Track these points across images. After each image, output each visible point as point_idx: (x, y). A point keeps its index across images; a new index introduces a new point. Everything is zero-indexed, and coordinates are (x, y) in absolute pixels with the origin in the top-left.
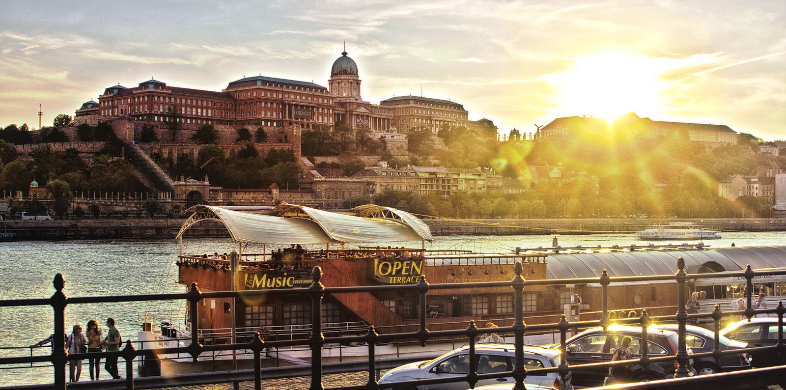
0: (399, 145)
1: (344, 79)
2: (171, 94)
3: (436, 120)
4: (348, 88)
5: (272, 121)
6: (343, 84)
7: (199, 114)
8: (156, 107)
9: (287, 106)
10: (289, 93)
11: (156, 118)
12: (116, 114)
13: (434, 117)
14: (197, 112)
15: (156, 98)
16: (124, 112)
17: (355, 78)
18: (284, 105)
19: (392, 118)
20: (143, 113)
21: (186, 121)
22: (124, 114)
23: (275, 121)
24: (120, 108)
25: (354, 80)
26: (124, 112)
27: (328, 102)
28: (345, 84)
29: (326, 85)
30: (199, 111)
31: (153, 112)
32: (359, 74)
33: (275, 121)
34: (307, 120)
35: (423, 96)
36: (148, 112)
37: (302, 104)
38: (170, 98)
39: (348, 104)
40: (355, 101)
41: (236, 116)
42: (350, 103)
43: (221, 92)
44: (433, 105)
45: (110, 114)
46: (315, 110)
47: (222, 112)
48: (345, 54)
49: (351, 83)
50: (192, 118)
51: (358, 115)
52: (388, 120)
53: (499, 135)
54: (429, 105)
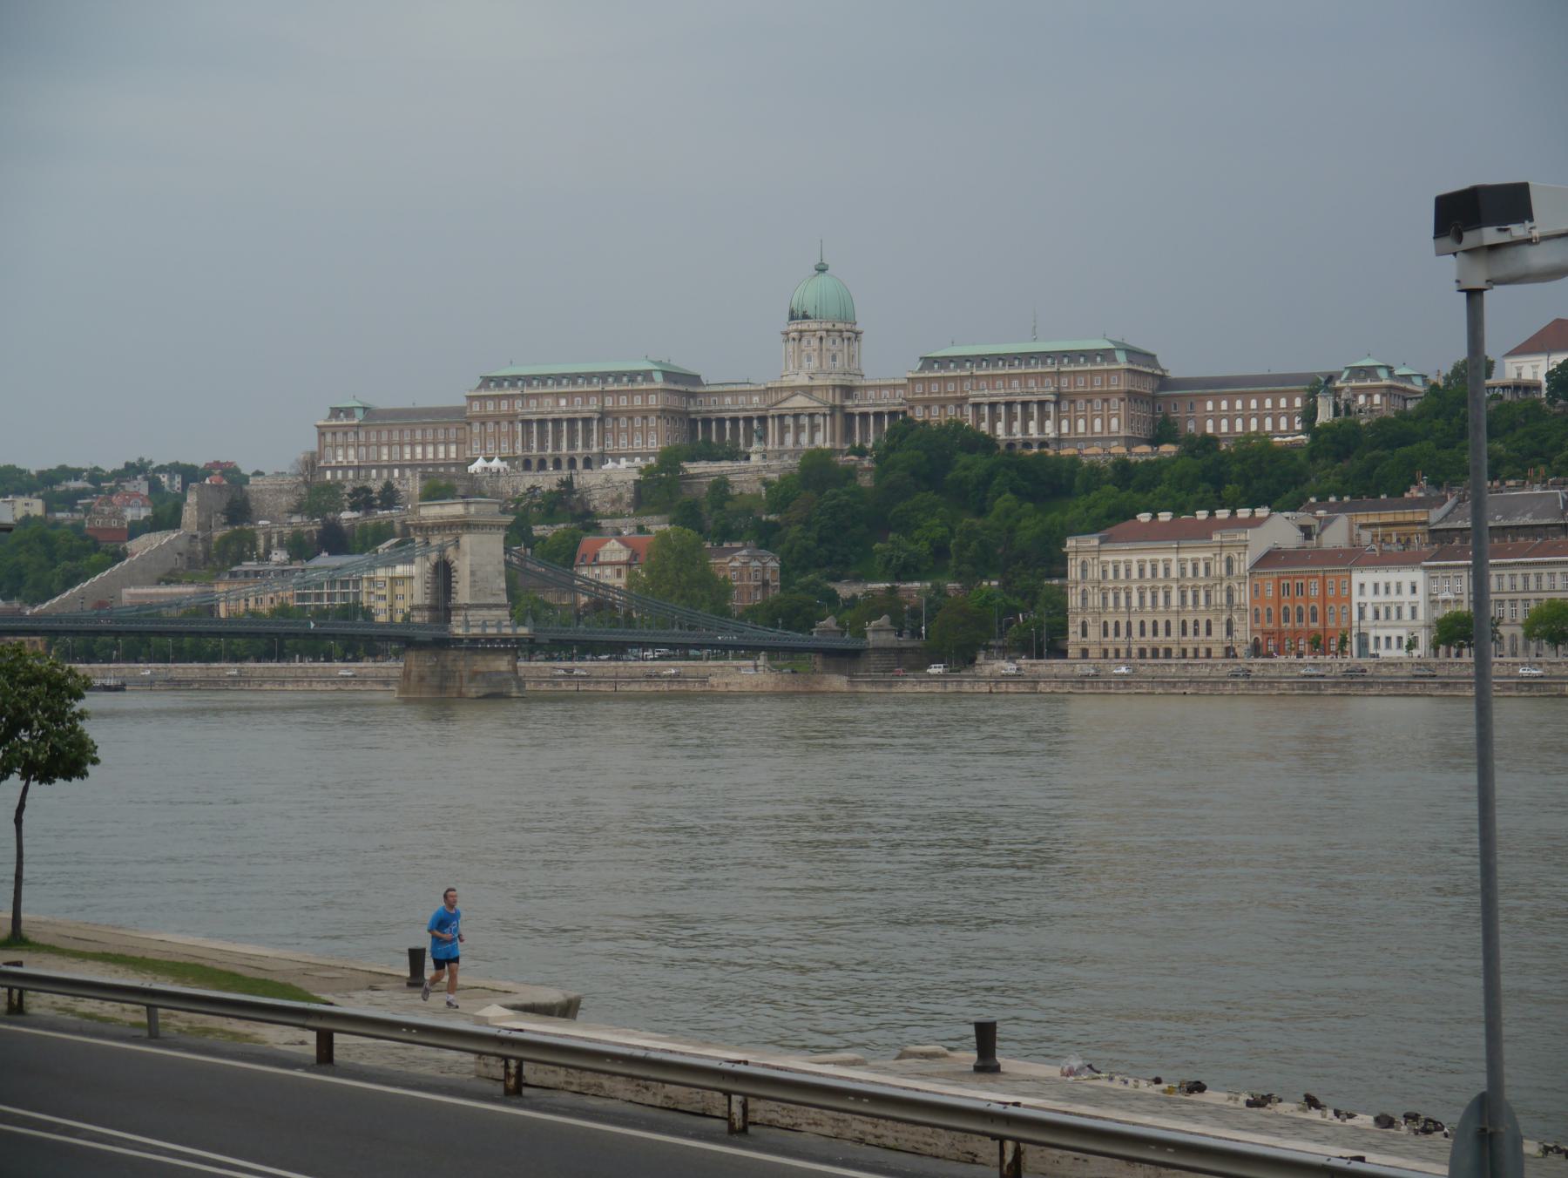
2: (358, 426)
14: (413, 453)
17: (814, 326)
38: (357, 434)
44: (979, 366)
50: (402, 467)
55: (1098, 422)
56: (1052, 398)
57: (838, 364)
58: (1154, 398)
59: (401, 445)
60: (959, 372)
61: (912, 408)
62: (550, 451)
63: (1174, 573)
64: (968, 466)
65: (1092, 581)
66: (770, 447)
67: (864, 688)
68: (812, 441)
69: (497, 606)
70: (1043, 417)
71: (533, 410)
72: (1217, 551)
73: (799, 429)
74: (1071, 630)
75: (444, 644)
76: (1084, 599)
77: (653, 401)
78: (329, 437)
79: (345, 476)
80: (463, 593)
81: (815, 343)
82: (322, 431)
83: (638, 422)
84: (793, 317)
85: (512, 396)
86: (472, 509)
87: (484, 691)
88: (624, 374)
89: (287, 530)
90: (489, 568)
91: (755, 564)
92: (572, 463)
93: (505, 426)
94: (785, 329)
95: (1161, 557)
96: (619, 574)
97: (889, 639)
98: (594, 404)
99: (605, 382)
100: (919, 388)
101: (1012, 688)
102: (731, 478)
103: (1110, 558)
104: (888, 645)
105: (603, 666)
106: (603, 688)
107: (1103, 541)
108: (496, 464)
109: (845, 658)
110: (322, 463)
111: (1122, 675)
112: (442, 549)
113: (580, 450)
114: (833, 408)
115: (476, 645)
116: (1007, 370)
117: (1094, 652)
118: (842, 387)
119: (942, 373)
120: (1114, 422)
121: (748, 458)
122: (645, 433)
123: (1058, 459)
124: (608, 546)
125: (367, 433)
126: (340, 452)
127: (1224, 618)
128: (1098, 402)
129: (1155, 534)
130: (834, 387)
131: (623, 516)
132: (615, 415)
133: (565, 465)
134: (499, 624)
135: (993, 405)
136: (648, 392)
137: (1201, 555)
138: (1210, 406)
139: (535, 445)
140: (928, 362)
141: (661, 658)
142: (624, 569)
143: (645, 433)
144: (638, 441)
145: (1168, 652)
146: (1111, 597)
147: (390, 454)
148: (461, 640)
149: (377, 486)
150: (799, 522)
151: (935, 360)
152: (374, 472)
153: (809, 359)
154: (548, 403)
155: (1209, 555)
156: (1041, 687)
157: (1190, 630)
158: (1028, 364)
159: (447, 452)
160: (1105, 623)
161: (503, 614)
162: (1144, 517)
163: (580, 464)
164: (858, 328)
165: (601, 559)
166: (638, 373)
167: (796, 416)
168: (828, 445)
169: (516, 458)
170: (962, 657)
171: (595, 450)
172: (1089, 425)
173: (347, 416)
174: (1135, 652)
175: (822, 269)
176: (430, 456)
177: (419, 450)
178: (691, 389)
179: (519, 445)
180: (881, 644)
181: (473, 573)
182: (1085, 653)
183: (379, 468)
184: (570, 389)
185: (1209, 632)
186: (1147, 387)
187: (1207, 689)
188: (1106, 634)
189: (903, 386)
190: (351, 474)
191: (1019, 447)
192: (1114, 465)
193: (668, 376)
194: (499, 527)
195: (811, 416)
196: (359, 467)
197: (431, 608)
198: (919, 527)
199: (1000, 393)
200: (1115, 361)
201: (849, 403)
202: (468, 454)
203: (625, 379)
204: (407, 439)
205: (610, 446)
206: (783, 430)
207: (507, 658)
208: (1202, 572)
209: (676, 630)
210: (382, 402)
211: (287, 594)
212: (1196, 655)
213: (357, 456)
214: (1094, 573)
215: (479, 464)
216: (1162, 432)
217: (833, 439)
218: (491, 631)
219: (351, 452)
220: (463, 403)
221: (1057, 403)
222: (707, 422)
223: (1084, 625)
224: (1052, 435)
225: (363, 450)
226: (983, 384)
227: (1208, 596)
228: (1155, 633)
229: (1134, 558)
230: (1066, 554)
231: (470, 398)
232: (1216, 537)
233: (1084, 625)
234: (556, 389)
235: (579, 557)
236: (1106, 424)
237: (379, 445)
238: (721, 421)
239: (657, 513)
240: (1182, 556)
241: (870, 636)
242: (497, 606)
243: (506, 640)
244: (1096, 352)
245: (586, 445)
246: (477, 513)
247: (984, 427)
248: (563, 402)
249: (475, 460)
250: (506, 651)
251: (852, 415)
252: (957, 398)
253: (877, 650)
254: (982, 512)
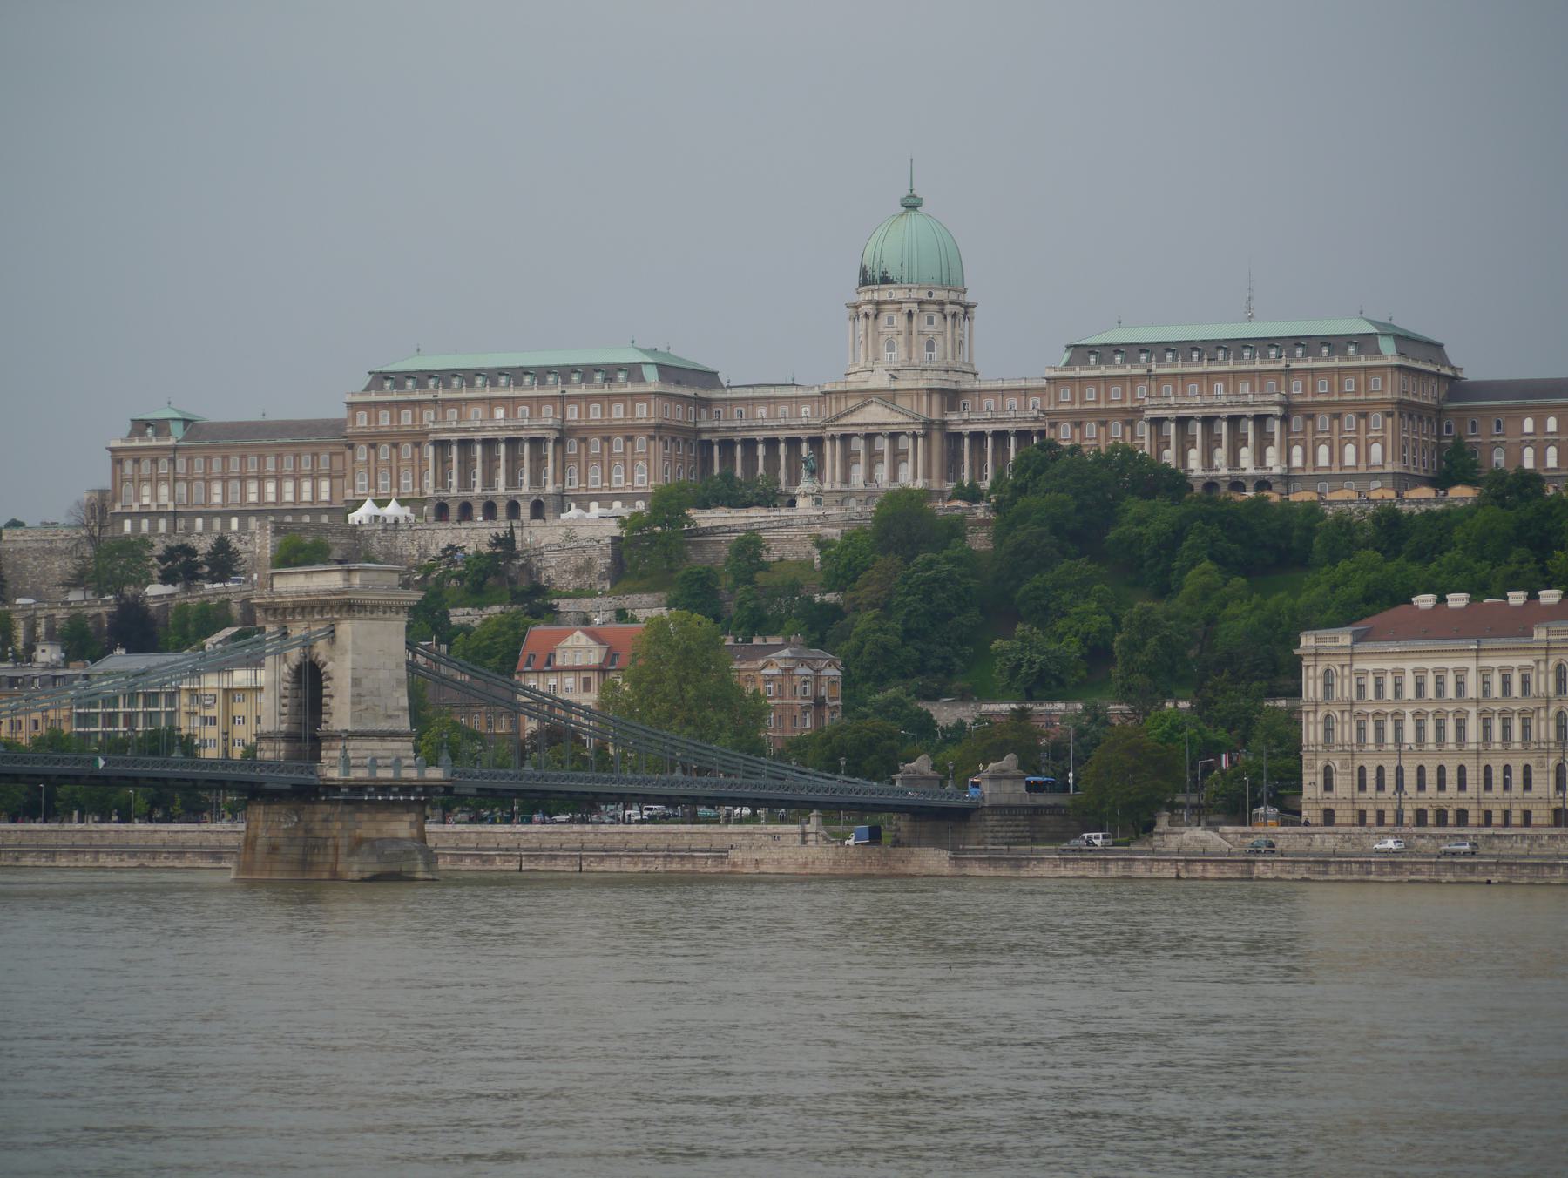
0: (581, 561)
2: (175, 449)
14: (261, 492)
17: (899, 295)
37: (489, 435)
38: (173, 461)
44: (1161, 360)
50: (243, 514)
55: (1350, 450)
56: (1277, 410)
57: (935, 354)
58: (1440, 412)
59: (243, 479)
60: (1129, 370)
61: (1054, 425)
62: (478, 490)
63: (1472, 690)
64: (1144, 518)
65: (1341, 701)
66: (827, 487)
67: (975, 869)
68: (894, 477)
69: (394, 735)
70: (1263, 441)
71: (451, 424)
72: (1541, 655)
73: (873, 458)
74: (1306, 779)
75: (308, 794)
76: (1328, 731)
77: (642, 412)
78: (128, 467)
79: (154, 527)
80: (340, 715)
81: (900, 321)
82: (117, 457)
83: (618, 444)
84: (865, 280)
85: (419, 403)
86: (356, 580)
87: (373, 868)
88: (596, 369)
89: (61, 614)
90: (383, 674)
91: (802, 670)
92: (513, 509)
93: (407, 450)
94: (855, 299)
95: (1450, 664)
96: (587, 685)
97: (1013, 792)
98: (549, 416)
99: (566, 381)
100: (1065, 394)
101: (1212, 871)
102: (765, 536)
103: (1370, 666)
104: (1015, 801)
105: (560, 832)
106: (560, 866)
107: (1359, 638)
108: (392, 510)
109: (946, 821)
110: (118, 508)
111: (1388, 852)
112: (307, 644)
113: (525, 489)
114: (928, 424)
115: (361, 797)
116: (1206, 367)
117: (1344, 815)
118: (942, 391)
119: (1103, 371)
120: (1376, 449)
121: (792, 504)
122: (630, 463)
123: (1287, 509)
124: (570, 642)
125: (189, 459)
126: (146, 490)
127: (1552, 762)
128: (1350, 419)
129: (1441, 628)
130: (930, 391)
131: (593, 595)
132: (582, 434)
133: (502, 512)
134: (397, 764)
135: (1182, 422)
136: (635, 397)
137: (1516, 662)
138: (1529, 425)
139: (455, 480)
140: (1081, 352)
141: (652, 820)
142: (594, 678)
143: (630, 463)
144: (618, 476)
145: (1462, 817)
146: (1371, 727)
147: (225, 494)
148: (336, 789)
149: (203, 545)
150: (874, 606)
151: (1091, 349)
152: (199, 522)
153: (891, 348)
154: (476, 414)
155: (1529, 662)
156: (1259, 869)
157: (1497, 780)
158: (1239, 357)
159: (315, 491)
160: (1362, 769)
161: (404, 747)
162: (1425, 601)
163: (525, 512)
164: (968, 299)
165: (559, 662)
166: (620, 368)
167: (870, 438)
168: (919, 484)
169: (424, 501)
170: (1135, 822)
171: (550, 489)
172: (1337, 455)
173: (157, 434)
174: (1409, 815)
175: (911, 205)
176: (289, 497)
177: (271, 487)
178: (703, 394)
179: (429, 481)
180: (1003, 800)
181: (356, 682)
182: (1329, 817)
183: (208, 515)
184: (511, 392)
185: (1527, 785)
186: (1428, 395)
187: (1525, 876)
188: (1362, 786)
189: (1040, 391)
190: (162, 525)
191: (1224, 488)
192: (1377, 519)
193: (666, 372)
194: (399, 609)
195: (894, 437)
196: (176, 515)
197: (289, 737)
198: (1065, 614)
199: (1194, 403)
200: (1378, 352)
201: (953, 417)
202: (349, 497)
203: (598, 377)
204: (252, 470)
205: (574, 484)
206: (848, 459)
207: (411, 817)
208: (1516, 690)
209: (678, 774)
210: (214, 411)
211: (61, 715)
212: (1507, 822)
213: (173, 495)
214: (1345, 688)
215: (365, 512)
216: (1453, 466)
217: (928, 475)
218: (385, 774)
219: (164, 490)
220: (342, 413)
221: (1285, 419)
222: (727, 446)
223: (1328, 772)
224: (1277, 470)
225: (182, 488)
226: (1167, 388)
227: (1526, 728)
228: (1441, 786)
229: (1409, 666)
230: (1300, 658)
231: (350, 405)
232: (1540, 634)
233: (1328, 772)
234: (488, 393)
235: (523, 659)
236: (1363, 454)
237: (208, 480)
238: (750, 445)
239: (647, 590)
240: (1484, 663)
241: (987, 787)
242: (394, 735)
243: (407, 789)
244: (1349, 339)
245: (536, 480)
246: (364, 586)
247: (1169, 456)
248: (500, 413)
249: (360, 503)
250: (407, 806)
251: (958, 436)
252: (1125, 410)
253: (996, 809)
254: (1164, 591)
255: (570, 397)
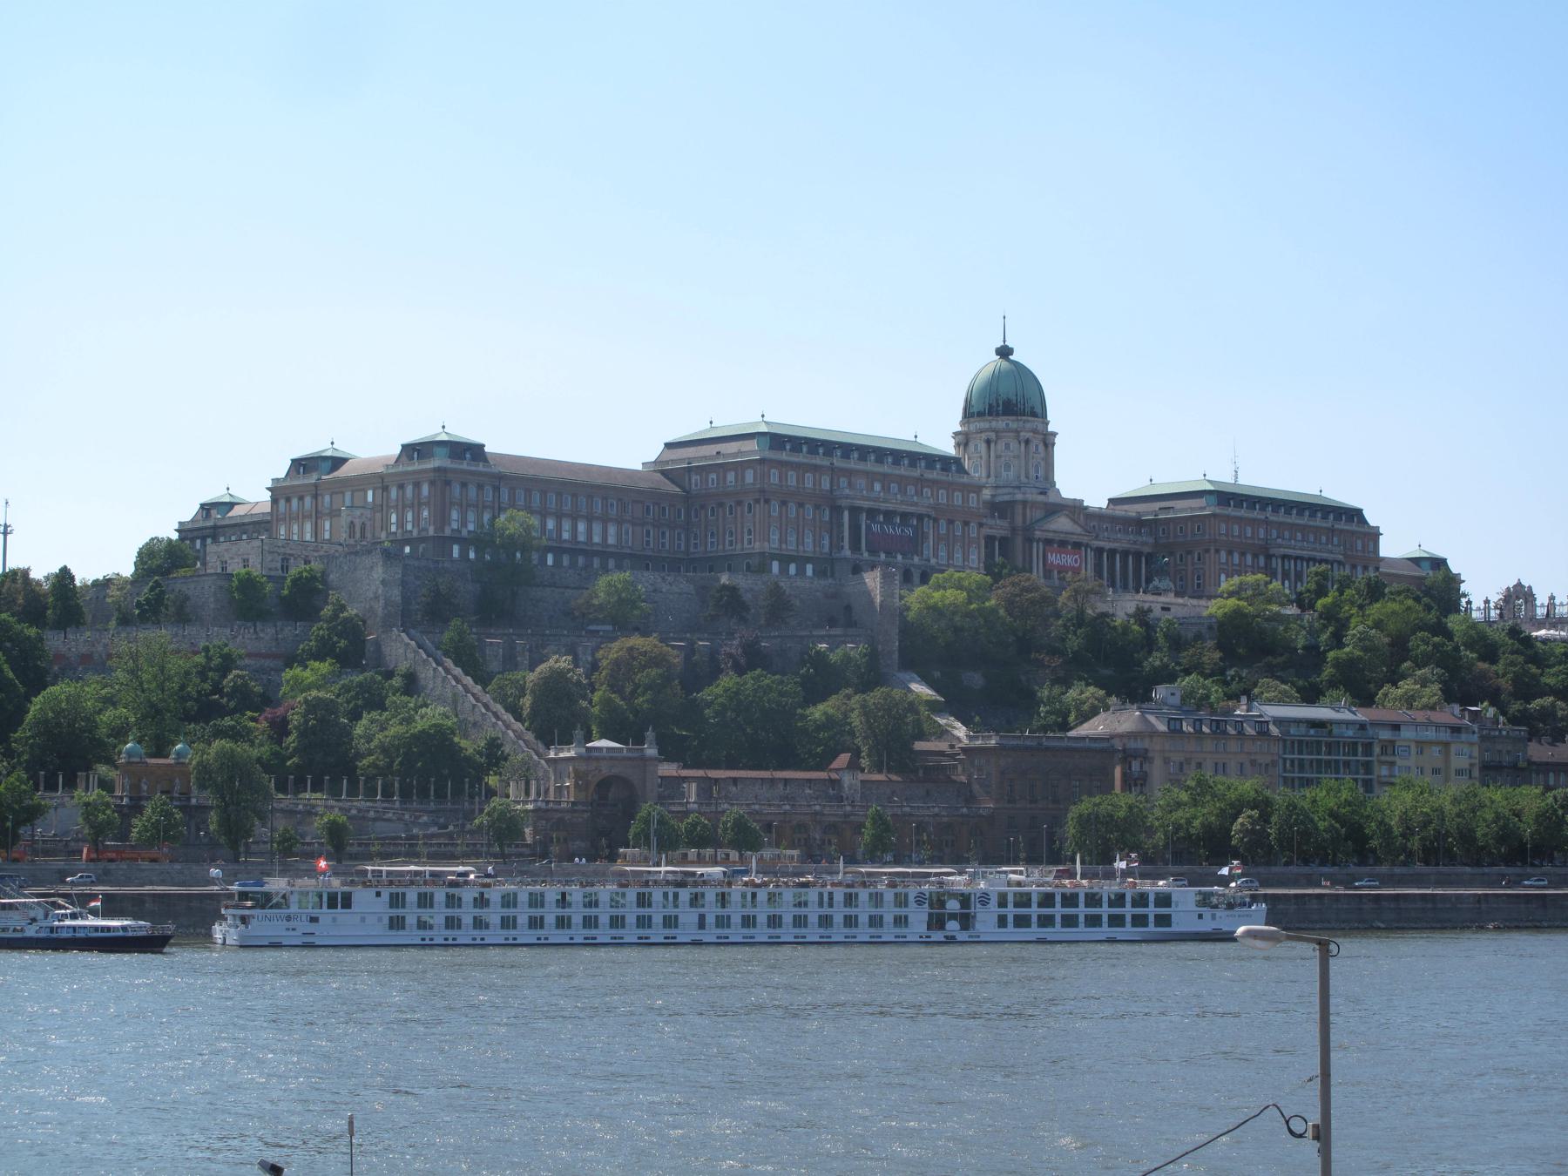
1: (1004, 431)
3: (1284, 557)
4: (1018, 457)
5: (802, 561)
6: (1001, 446)
7: (581, 538)
8: (455, 515)
9: (846, 513)
10: (850, 473)
11: (456, 550)
12: (327, 536)
13: (1280, 546)
15: (457, 490)
16: (358, 529)
17: (1040, 427)
18: (836, 510)
19: (1147, 550)
20: (415, 534)
21: (543, 561)
22: (358, 535)
23: (809, 560)
24: (344, 520)
25: (1035, 431)
26: (358, 529)
27: (965, 499)
28: (1007, 446)
29: (948, 447)
30: (581, 527)
31: (448, 532)
32: (1051, 415)
33: (809, 560)
34: (904, 555)
35: (1241, 481)
36: (431, 532)
38: (496, 489)
39: (1019, 509)
40: (1041, 498)
41: (687, 546)
42: (1024, 503)
43: (640, 468)
45: (308, 537)
46: (928, 527)
47: (648, 533)
48: (1004, 352)
49: (1027, 442)
50: (558, 551)
51: (1048, 542)
52: (1137, 555)
53: (1469, 602)
54: (1263, 509)
255: (928, 480)
